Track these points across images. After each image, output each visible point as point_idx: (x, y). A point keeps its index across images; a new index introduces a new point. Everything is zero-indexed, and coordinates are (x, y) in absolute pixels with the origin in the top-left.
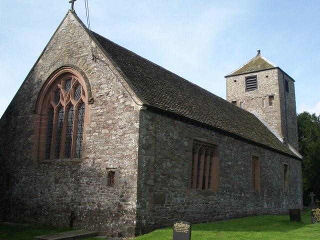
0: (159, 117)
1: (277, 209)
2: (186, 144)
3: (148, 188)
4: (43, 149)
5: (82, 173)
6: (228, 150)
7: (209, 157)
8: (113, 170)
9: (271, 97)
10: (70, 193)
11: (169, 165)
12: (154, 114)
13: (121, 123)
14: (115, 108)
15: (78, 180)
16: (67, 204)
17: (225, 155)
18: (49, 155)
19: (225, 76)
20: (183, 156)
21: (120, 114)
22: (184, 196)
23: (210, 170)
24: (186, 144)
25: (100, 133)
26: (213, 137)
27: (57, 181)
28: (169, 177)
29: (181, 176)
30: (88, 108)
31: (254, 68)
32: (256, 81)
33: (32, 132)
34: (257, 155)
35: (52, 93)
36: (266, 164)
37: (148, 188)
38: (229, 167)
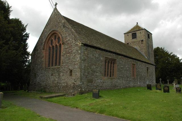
0: (89, 48)
1: (144, 85)
2: (102, 59)
3: (85, 76)
4: (47, 63)
5: (61, 71)
6: (120, 60)
7: (112, 64)
8: (72, 70)
9: (142, 41)
10: (56, 79)
11: (94, 67)
12: (87, 47)
13: (74, 51)
14: (72, 45)
15: (59, 74)
16: (55, 84)
17: (120, 63)
18: (49, 65)
19: (125, 33)
20: (101, 64)
21: (74, 48)
22: (102, 79)
23: (113, 69)
24: (102, 59)
25: (66, 56)
26: (114, 56)
27: (52, 75)
28: (95, 72)
29: (100, 71)
30: (62, 46)
31: (135, 30)
32: (136, 35)
33: (43, 57)
34: (134, 63)
35: (50, 42)
36: (139, 67)
37: (85, 76)
38: (122, 68)
